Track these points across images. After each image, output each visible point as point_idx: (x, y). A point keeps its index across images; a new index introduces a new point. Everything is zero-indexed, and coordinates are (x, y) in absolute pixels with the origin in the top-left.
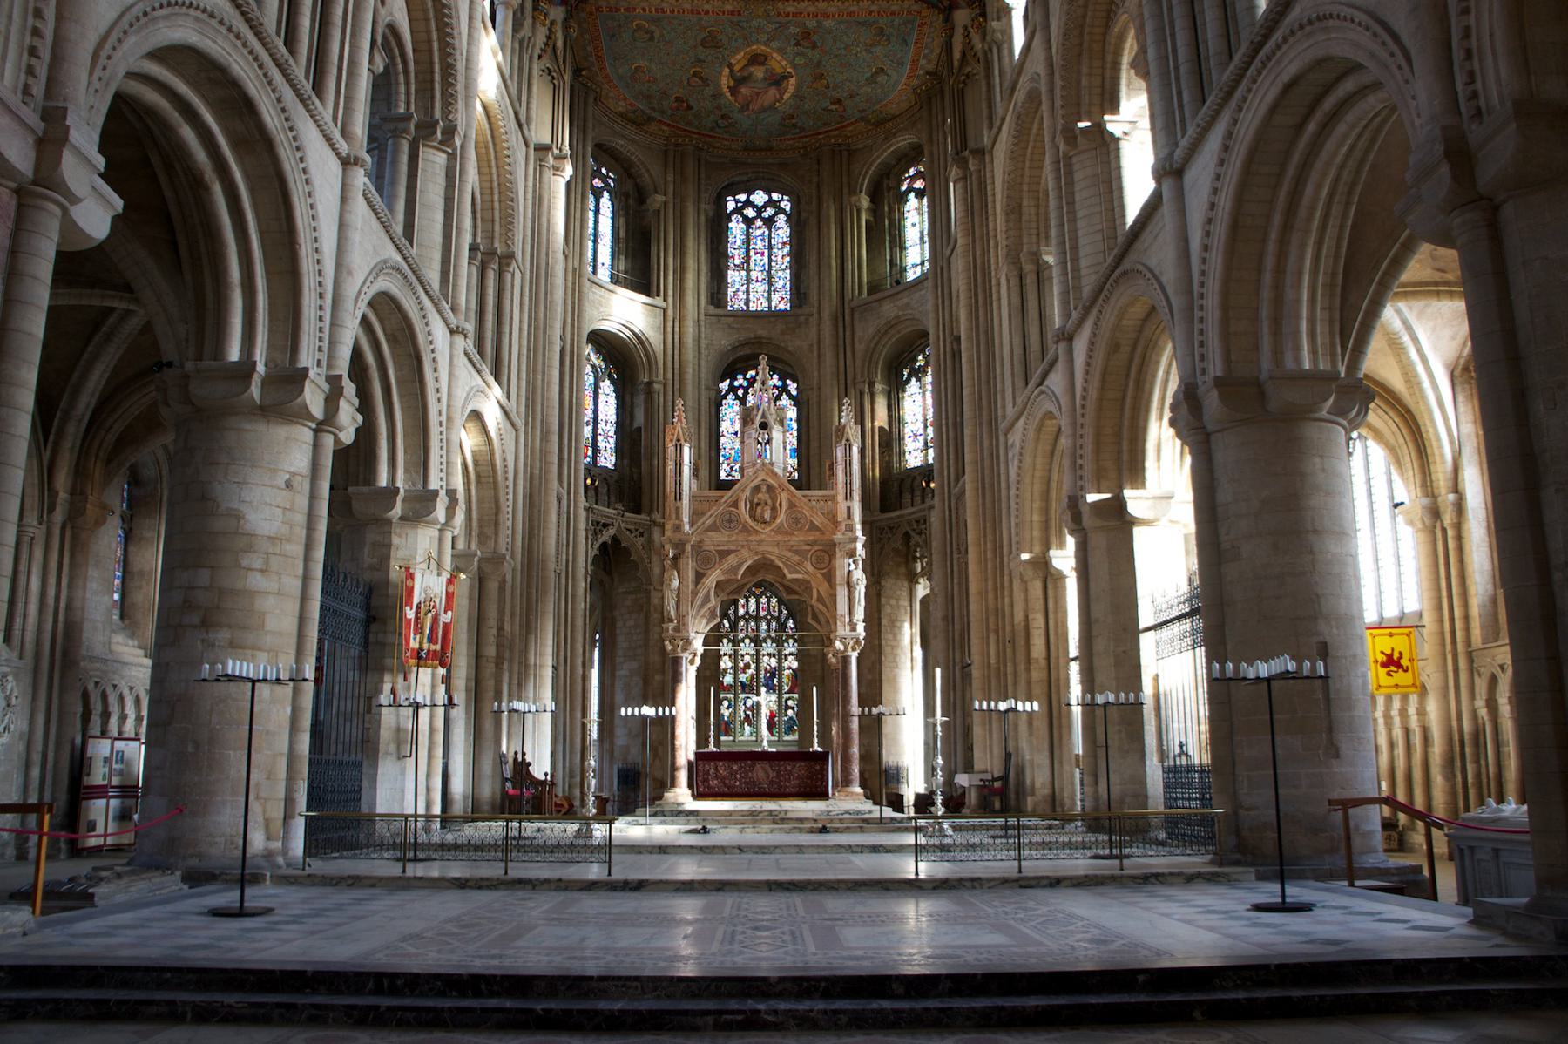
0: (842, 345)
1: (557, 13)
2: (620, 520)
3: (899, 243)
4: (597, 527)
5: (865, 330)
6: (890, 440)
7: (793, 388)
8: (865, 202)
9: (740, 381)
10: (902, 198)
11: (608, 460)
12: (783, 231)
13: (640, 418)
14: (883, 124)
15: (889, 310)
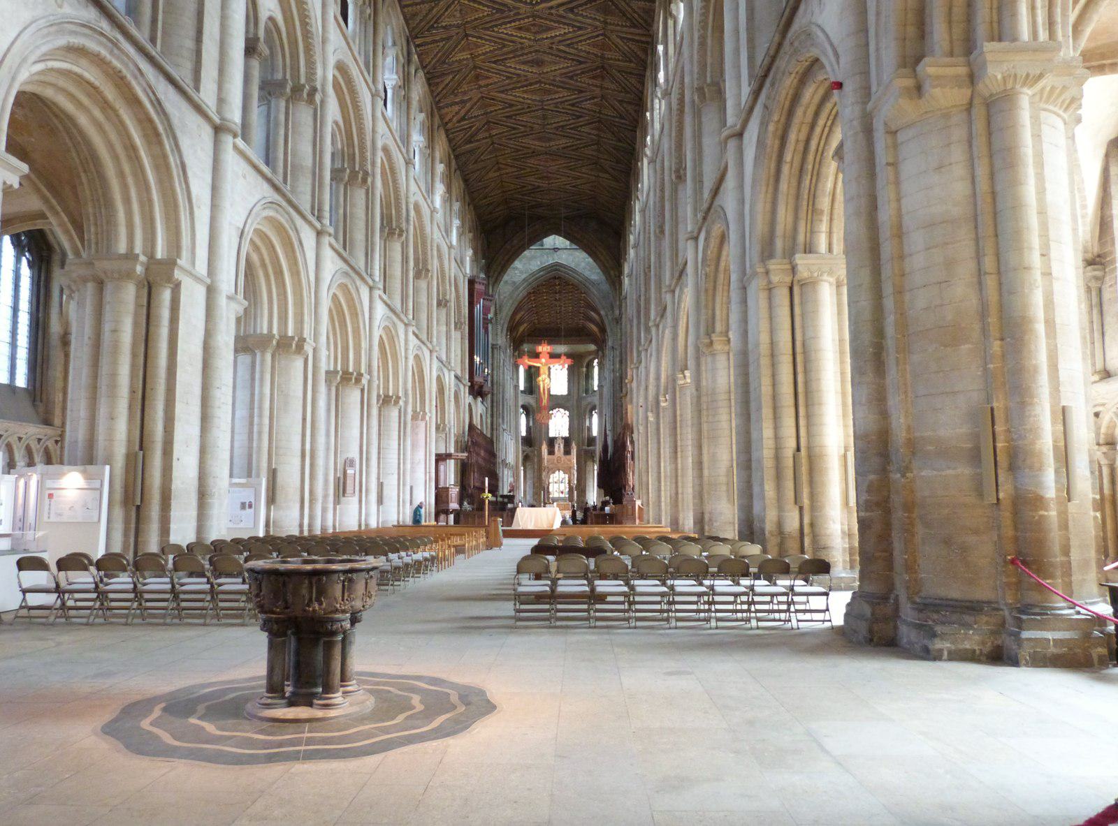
0: (579, 407)
1: (516, 354)
2: (528, 449)
3: (593, 378)
4: (523, 452)
5: (584, 403)
6: (590, 429)
7: (567, 413)
8: (584, 369)
9: (555, 411)
10: (594, 367)
11: (524, 433)
12: (565, 372)
13: (531, 424)
14: (590, 353)
15: (589, 399)
